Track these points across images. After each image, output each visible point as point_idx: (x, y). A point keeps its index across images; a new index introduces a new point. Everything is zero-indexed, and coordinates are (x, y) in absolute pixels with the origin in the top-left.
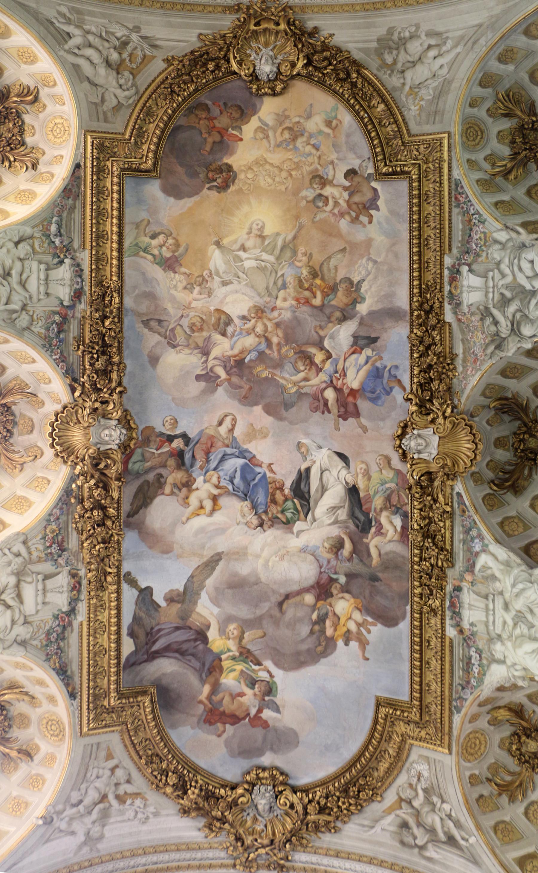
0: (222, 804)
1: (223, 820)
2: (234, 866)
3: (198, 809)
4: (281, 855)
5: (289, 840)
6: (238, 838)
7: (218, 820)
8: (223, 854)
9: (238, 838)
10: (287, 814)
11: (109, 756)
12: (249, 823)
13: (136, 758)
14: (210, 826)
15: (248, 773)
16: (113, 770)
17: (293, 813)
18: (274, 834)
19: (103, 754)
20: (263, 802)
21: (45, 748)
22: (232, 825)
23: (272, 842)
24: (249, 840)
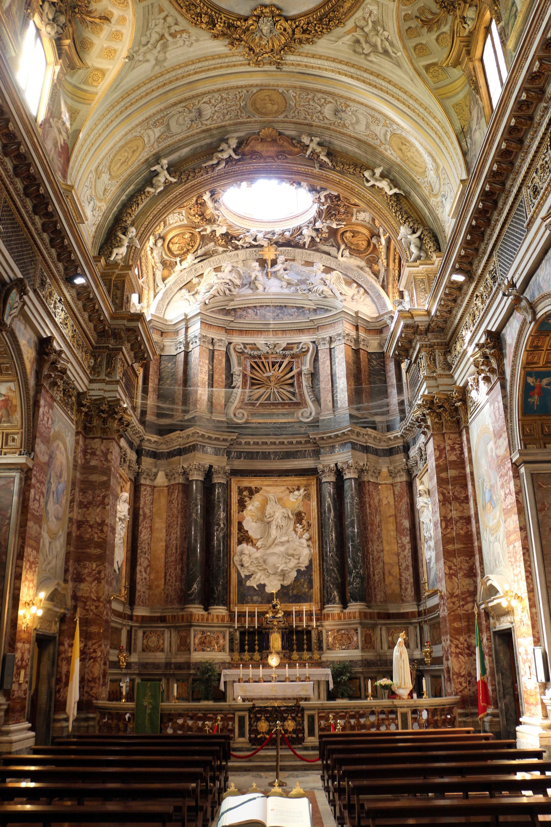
0: (239, 31)
1: (240, 40)
2: (249, 64)
3: (224, 34)
4: (278, 57)
5: (283, 49)
6: (251, 49)
7: (237, 40)
8: (242, 58)
9: (251, 49)
10: (281, 34)
11: (161, 10)
12: (257, 40)
13: (179, 8)
14: (232, 44)
15: (255, 9)
16: (165, 19)
17: (285, 33)
18: (273, 46)
19: (156, 10)
20: (266, 28)
21: (116, 12)
22: (246, 42)
23: (272, 50)
24: (257, 50)
